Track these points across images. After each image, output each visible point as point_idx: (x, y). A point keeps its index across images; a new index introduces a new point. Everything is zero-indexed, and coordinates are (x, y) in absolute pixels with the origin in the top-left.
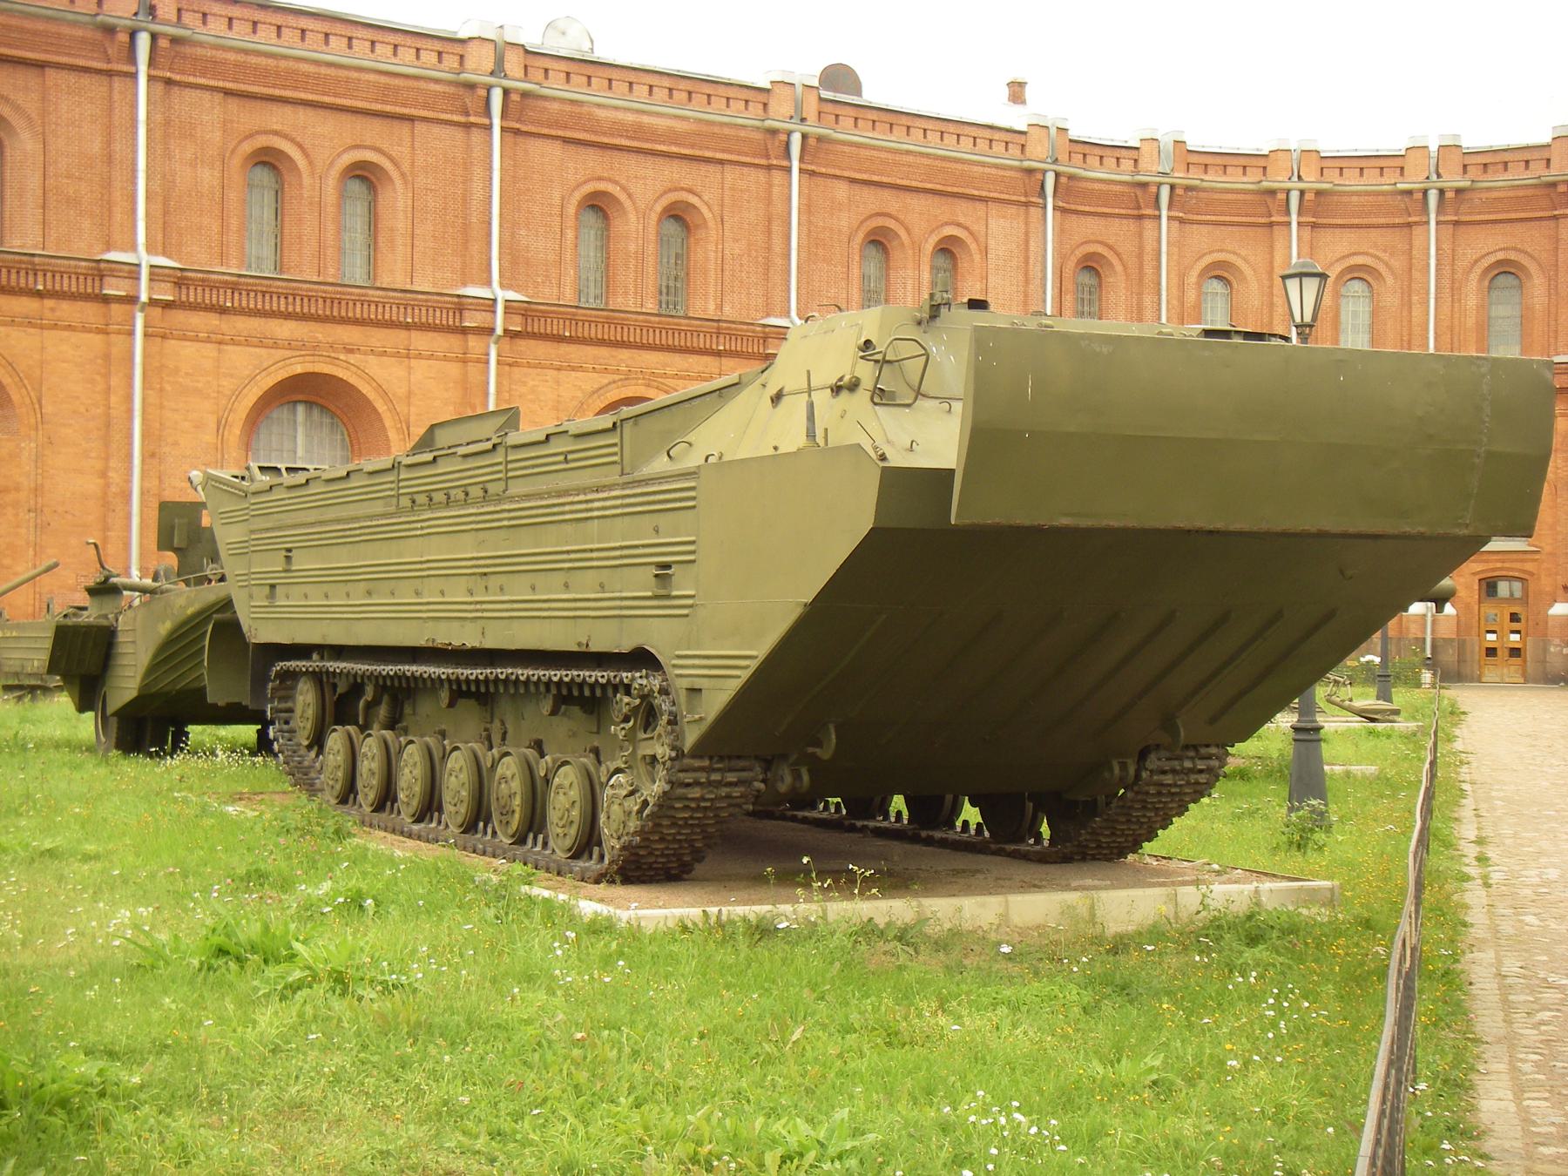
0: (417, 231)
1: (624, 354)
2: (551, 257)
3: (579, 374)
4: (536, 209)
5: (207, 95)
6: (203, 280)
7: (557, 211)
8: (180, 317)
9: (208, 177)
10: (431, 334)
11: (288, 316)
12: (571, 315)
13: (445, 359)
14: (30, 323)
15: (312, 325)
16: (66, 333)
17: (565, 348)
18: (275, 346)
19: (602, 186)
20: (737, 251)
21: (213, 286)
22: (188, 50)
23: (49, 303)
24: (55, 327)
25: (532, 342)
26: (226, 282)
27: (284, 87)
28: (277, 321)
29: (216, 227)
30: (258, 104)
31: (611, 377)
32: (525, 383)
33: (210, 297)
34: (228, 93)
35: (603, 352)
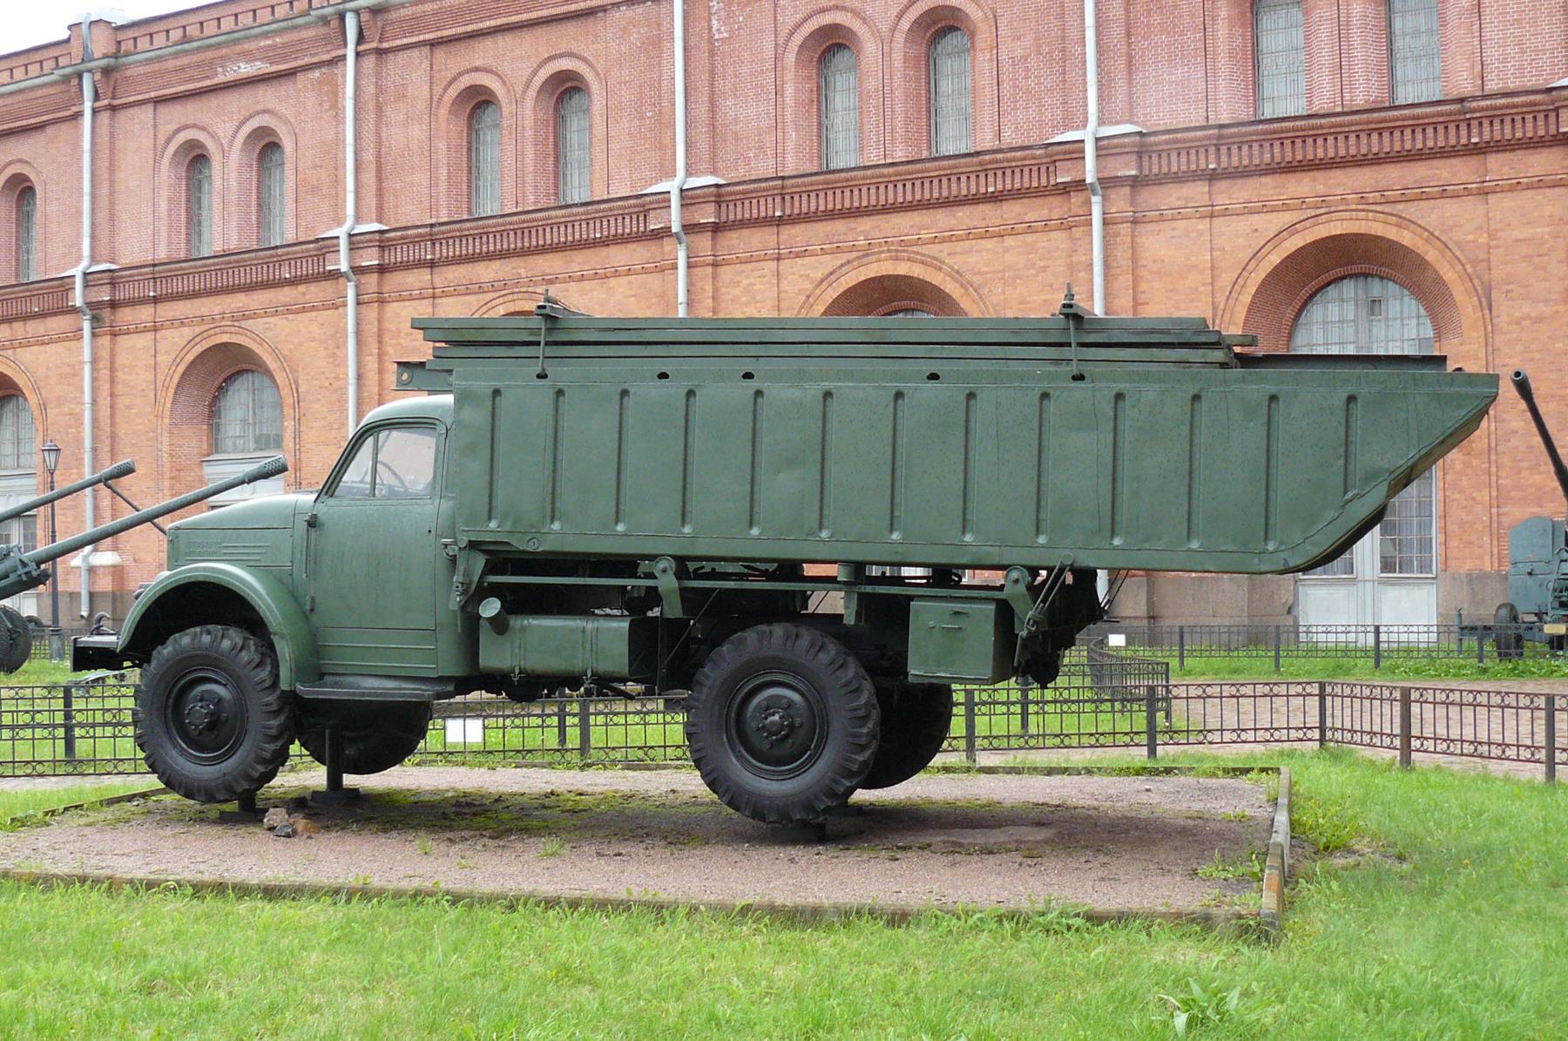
0: (612, 133)
1: (866, 224)
2: (765, 123)
3: (806, 260)
4: (745, 69)
5: (415, 53)
6: (403, 238)
7: (770, 64)
8: (397, 280)
9: (418, 132)
10: (631, 246)
11: (489, 257)
12: (781, 186)
13: (644, 271)
14: (289, 310)
15: (515, 262)
16: (314, 314)
17: (788, 232)
18: (481, 291)
19: (827, 19)
20: (1019, 52)
21: (416, 241)
22: (393, 15)
23: (302, 288)
24: (304, 310)
25: (746, 232)
26: (420, 235)
27: (481, 20)
28: (482, 264)
29: (426, 182)
30: (462, 45)
31: (845, 257)
32: (738, 284)
33: (414, 253)
34: (433, 44)
35: (839, 226)
